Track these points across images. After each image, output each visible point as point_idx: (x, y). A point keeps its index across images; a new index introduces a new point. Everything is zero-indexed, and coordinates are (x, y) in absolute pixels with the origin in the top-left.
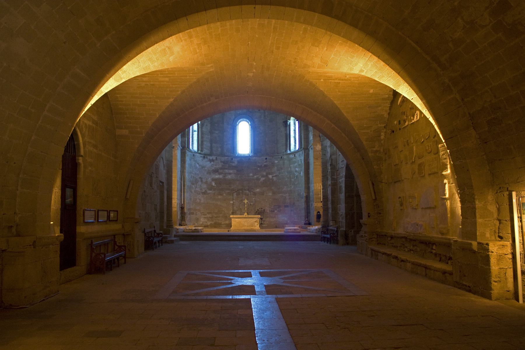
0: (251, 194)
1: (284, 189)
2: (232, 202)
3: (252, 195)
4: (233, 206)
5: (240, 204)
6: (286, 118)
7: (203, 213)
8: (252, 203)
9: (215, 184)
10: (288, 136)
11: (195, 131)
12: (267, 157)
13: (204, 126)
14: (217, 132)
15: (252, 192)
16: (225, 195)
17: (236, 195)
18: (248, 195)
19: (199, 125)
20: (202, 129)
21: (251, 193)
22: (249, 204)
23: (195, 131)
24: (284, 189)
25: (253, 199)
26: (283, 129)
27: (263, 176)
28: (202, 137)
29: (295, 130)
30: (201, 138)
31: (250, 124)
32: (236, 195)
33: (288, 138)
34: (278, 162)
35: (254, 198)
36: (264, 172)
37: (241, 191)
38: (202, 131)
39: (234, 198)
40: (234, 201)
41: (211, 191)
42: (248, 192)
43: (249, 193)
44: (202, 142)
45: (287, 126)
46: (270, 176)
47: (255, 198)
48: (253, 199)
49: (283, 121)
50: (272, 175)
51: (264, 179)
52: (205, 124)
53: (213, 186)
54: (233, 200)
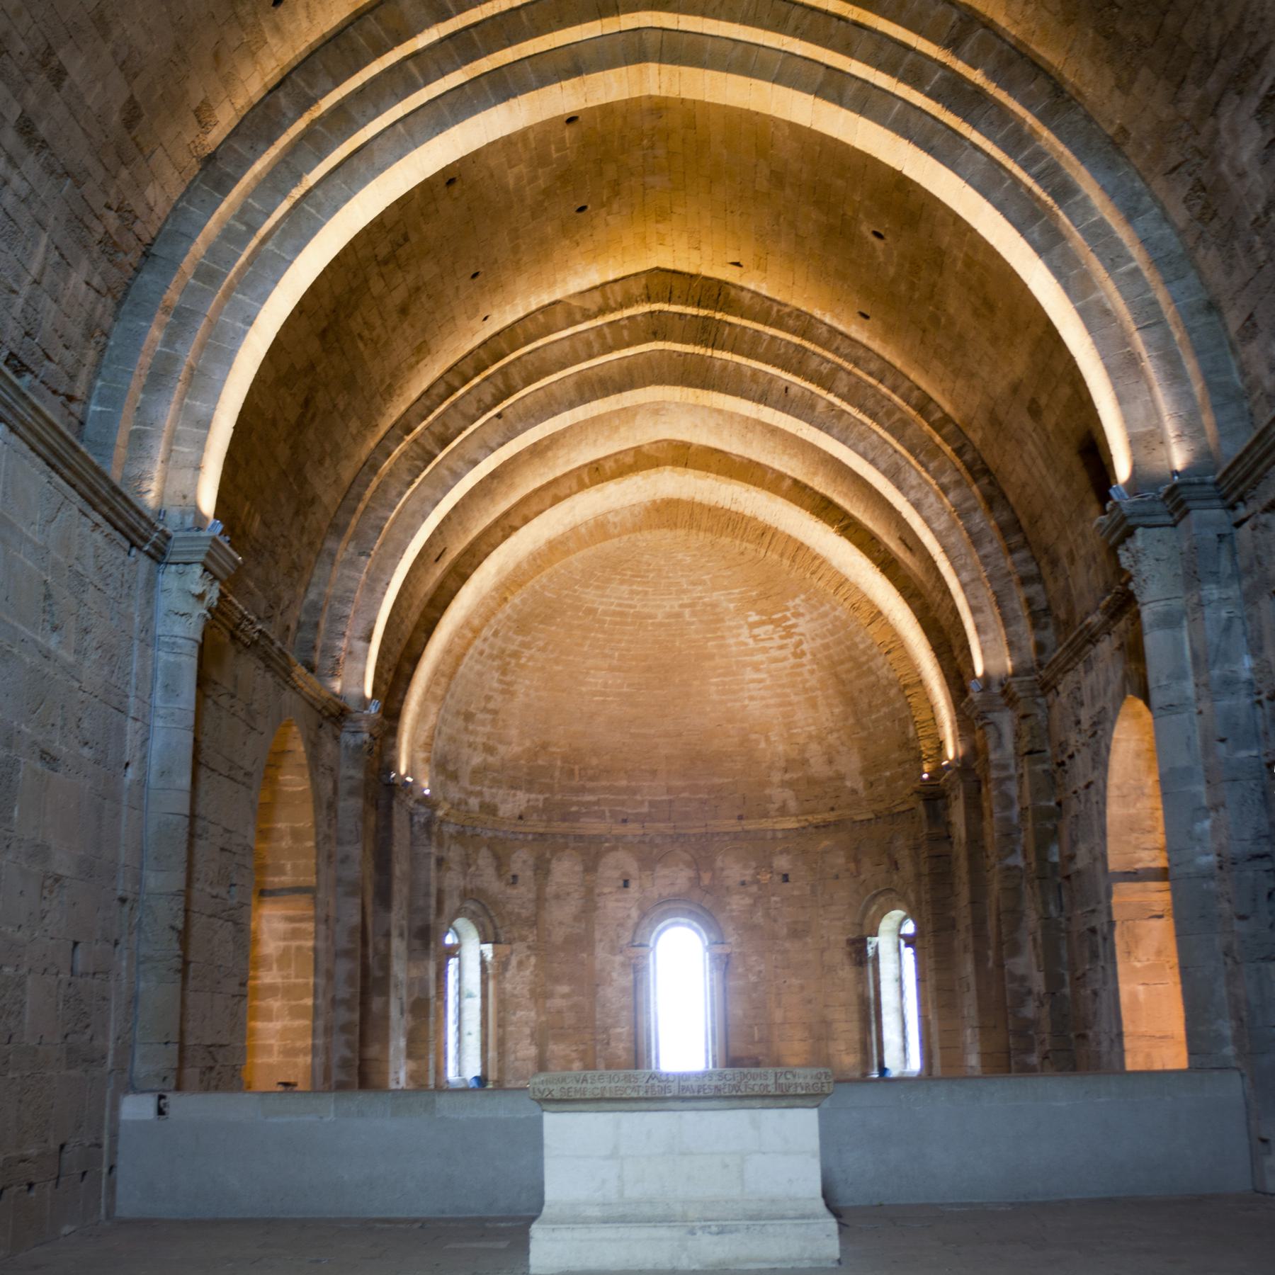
6: (861, 925)
10: (872, 1007)
11: (470, 996)
13: (510, 967)
14: (565, 989)
19: (489, 967)
20: (499, 983)
23: (470, 996)
26: (847, 972)
28: (501, 1024)
29: (900, 980)
30: (499, 1026)
33: (873, 1019)
38: (500, 992)
44: (501, 1042)
45: (866, 962)
49: (845, 938)
52: (514, 961)
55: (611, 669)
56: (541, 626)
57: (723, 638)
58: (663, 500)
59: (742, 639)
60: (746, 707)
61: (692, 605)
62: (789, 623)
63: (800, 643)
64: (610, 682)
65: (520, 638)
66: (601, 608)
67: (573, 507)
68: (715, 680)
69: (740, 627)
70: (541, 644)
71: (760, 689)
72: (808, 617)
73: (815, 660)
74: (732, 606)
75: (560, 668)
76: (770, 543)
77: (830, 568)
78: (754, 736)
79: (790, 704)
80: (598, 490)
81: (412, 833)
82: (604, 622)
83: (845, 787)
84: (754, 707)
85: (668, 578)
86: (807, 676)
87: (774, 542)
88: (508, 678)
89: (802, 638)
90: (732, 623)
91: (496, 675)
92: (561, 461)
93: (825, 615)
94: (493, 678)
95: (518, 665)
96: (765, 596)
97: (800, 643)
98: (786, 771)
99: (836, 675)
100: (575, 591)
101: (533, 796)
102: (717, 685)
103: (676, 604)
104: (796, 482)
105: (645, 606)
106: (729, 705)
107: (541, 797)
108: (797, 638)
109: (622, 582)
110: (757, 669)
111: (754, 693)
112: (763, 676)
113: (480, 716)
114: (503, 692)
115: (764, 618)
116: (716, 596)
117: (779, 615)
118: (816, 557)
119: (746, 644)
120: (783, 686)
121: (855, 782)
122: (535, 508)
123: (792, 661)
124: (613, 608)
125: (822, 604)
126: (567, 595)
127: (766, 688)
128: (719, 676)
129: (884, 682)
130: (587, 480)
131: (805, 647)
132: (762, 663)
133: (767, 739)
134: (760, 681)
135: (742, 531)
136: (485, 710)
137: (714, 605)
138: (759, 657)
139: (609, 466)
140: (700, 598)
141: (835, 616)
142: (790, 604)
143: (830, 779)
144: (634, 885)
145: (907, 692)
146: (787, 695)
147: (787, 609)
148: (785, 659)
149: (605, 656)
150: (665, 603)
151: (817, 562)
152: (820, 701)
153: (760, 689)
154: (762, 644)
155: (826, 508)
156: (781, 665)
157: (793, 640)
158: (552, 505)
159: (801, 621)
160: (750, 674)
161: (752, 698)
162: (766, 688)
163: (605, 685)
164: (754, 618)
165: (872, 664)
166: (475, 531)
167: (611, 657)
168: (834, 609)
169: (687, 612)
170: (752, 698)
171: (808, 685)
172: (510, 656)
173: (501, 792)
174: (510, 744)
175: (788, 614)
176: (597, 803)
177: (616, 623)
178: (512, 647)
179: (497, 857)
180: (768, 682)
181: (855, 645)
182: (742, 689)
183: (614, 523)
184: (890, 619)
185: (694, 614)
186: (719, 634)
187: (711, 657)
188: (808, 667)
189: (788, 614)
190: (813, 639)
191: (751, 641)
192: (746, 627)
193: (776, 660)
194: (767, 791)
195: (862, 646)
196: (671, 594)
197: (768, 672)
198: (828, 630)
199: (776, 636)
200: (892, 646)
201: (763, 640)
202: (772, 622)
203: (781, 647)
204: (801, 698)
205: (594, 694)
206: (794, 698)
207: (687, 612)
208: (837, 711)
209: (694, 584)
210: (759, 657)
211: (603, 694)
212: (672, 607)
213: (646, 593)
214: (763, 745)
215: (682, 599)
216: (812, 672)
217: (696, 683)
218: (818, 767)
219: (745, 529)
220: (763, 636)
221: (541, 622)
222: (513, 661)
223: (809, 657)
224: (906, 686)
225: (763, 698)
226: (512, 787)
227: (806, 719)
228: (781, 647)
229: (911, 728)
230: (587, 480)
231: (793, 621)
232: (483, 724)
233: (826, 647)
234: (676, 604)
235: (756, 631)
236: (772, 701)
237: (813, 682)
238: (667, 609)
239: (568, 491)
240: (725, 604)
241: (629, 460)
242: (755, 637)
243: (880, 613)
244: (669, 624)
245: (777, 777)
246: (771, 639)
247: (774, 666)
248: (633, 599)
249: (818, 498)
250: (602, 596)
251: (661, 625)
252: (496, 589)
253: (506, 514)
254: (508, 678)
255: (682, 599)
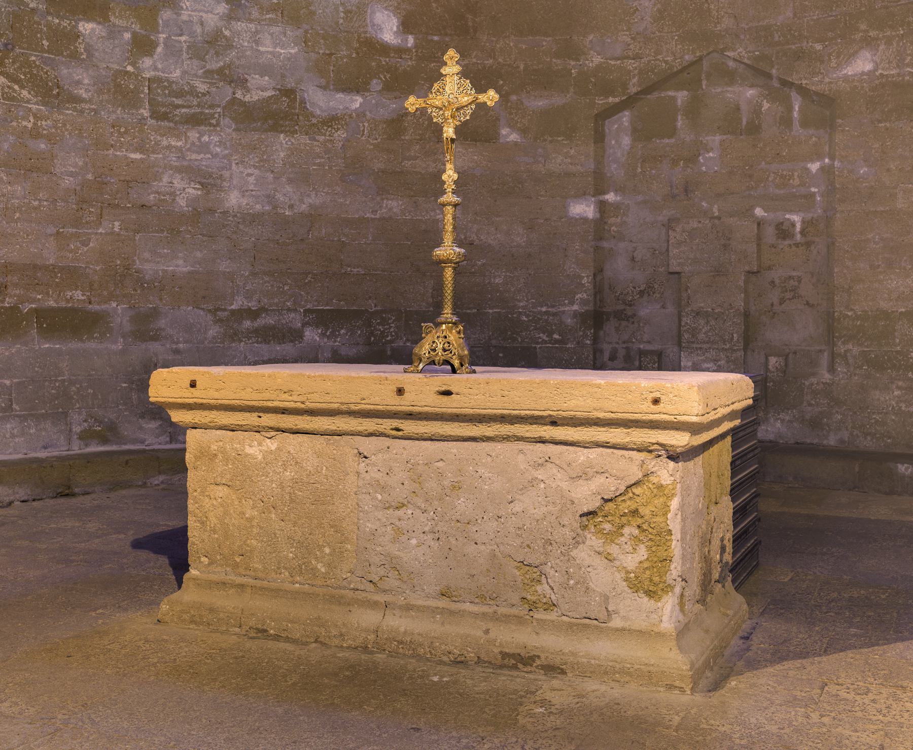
0: (786, 121)
2: (584, 209)
3: (797, 129)
4: (597, 249)
5: (669, 225)
7: (254, 314)
8: (796, 218)
9: (406, 26)
15: (803, 91)
16: (514, 137)
17: (635, 130)
18: (754, 129)
21: (790, 109)
22: (760, 223)
25: (814, 167)
32: (626, 141)
35: (820, 157)
37: (681, 96)
39: (614, 170)
40: (611, 197)
41: (357, 102)
42: (751, 92)
43: (766, 105)
47: (832, 158)
48: (814, 167)
53: (385, 49)
54: (599, 191)
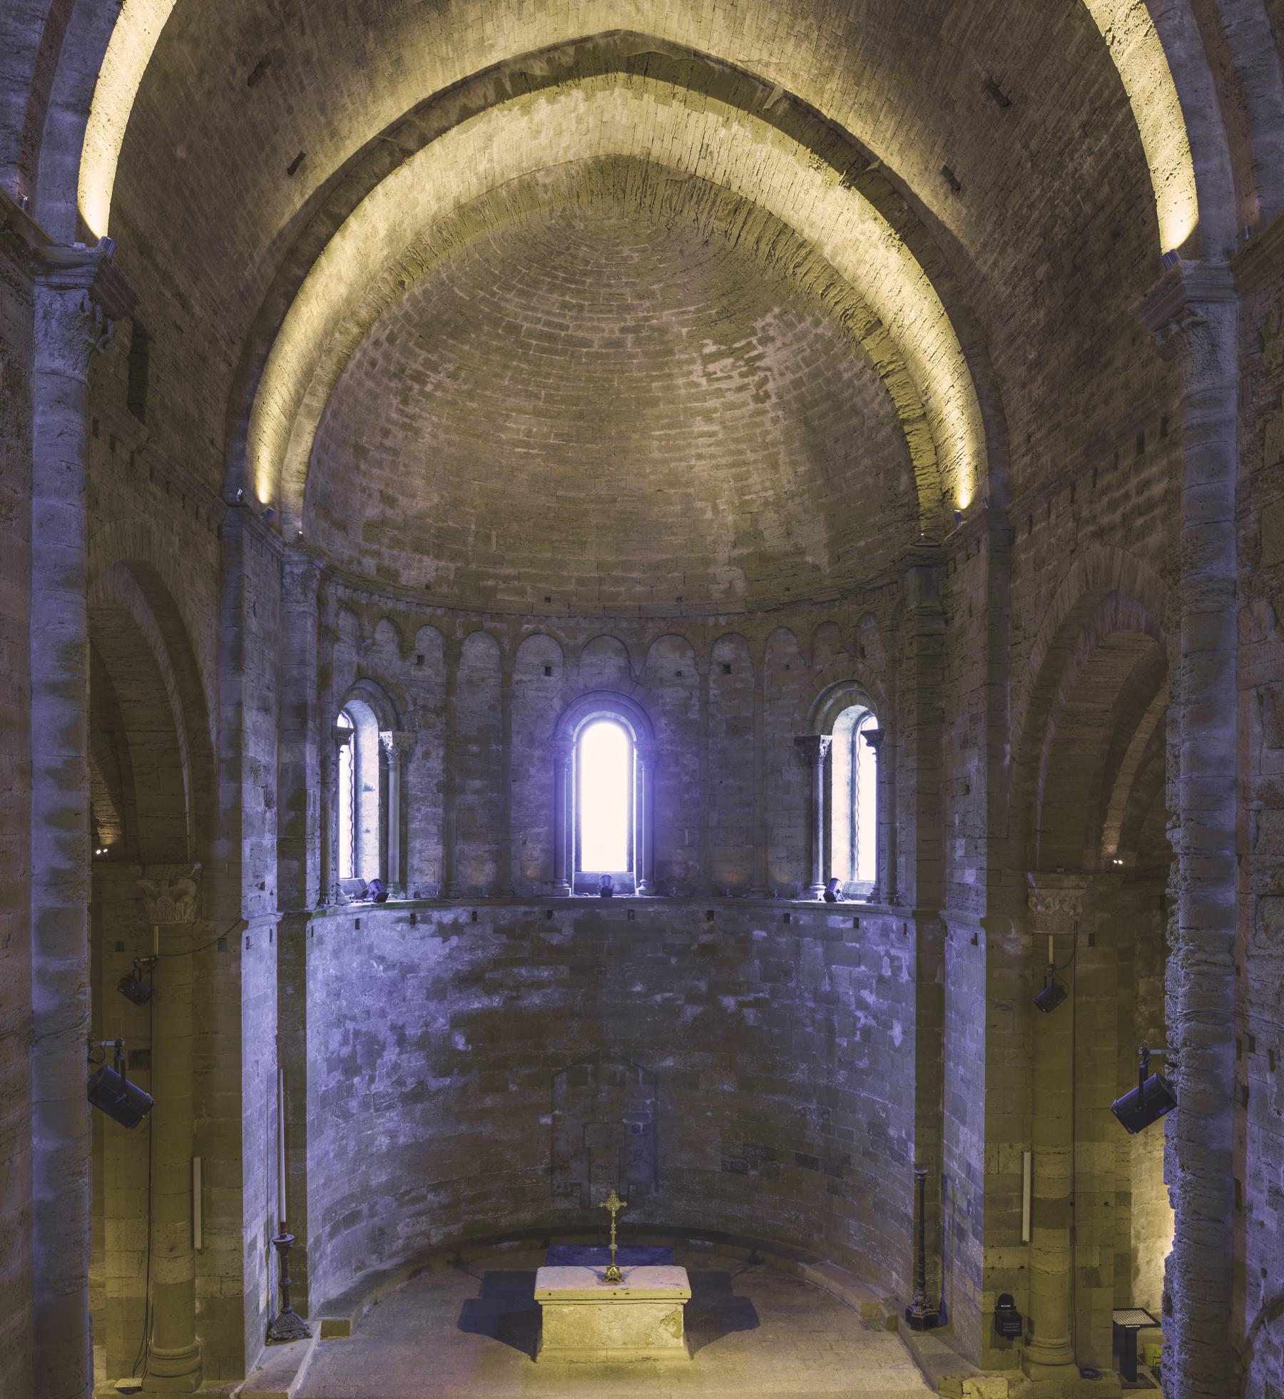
1: (799, 1076)
12: (717, 909)
24: (799, 1076)
27: (693, 998)
31: (635, 740)
34: (769, 938)
36: (698, 980)
46: (730, 1002)
50: (740, 998)
51: (698, 1010)
55: (537, 413)
56: (451, 341)
57: (670, 376)
58: (608, 156)
59: (694, 378)
60: (692, 467)
61: (635, 330)
62: (755, 353)
63: (765, 381)
64: (535, 430)
65: (424, 354)
66: (526, 325)
67: (489, 138)
68: (658, 433)
69: (692, 361)
70: (451, 367)
71: (710, 445)
72: (779, 343)
73: (781, 405)
74: (684, 331)
75: (474, 405)
76: (744, 223)
77: (821, 259)
78: (699, 504)
79: (745, 463)
80: (526, 110)
81: (282, 586)
82: (529, 346)
83: (806, 563)
84: (701, 467)
85: (609, 285)
86: (769, 426)
87: (750, 222)
88: (410, 410)
89: (768, 373)
90: (684, 357)
91: (395, 402)
92: (471, 36)
93: (803, 335)
94: (391, 405)
95: (422, 392)
96: (726, 314)
97: (765, 381)
98: (734, 546)
99: (806, 422)
100: (493, 294)
101: (442, 564)
102: (659, 439)
103: (616, 327)
104: (795, 102)
105: (579, 327)
106: (673, 465)
107: (452, 566)
108: (762, 374)
109: (552, 288)
110: (707, 416)
111: (703, 450)
112: (715, 428)
113: (377, 455)
114: (404, 427)
115: (723, 347)
116: (667, 316)
117: (743, 342)
118: (802, 245)
119: (697, 385)
120: (737, 441)
121: (818, 557)
122: (436, 125)
123: (752, 406)
124: (539, 327)
125: (801, 319)
126: (483, 299)
127: (718, 444)
128: (663, 427)
129: (871, 423)
130: (508, 87)
131: (770, 386)
132: (715, 410)
133: (715, 508)
134: (711, 434)
135: (709, 203)
136: (381, 447)
137: (663, 330)
138: (712, 403)
139: (539, 69)
140: (646, 319)
141: (816, 335)
142: (759, 324)
143: (787, 554)
144: (557, 673)
145: (907, 428)
146: (741, 452)
147: (754, 333)
148: (745, 404)
149: (530, 395)
150: (603, 325)
151: (803, 252)
152: (782, 457)
153: (710, 445)
154: (716, 385)
155: (833, 145)
156: (737, 412)
157: (756, 378)
158: (458, 122)
159: (770, 348)
160: (700, 426)
161: (700, 457)
162: (718, 444)
163: (529, 433)
164: (711, 348)
165: (858, 400)
166: (351, 147)
167: (537, 397)
168: (817, 323)
169: (630, 337)
170: (700, 457)
171: (769, 438)
172: (413, 378)
173: (403, 554)
174: (414, 497)
175: (754, 340)
176: (518, 577)
177: (544, 351)
178: (416, 366)
179: (399, 632)
180: (721, 436)
181: (838, 375)
182: (689, 445)
183: (545, 186)
184: (894, 331)
185: (638, 342)
186: (667, 371)
187: (655, 402)
188: (772, 414)
189: (754, 340)
190: (782, 374)
191: (704, 381)
192: (699, 361)
193: (731, 406)
194: (711, 571)
195: (846, 376)
196: (610, 311)
197: (722, 423)
198: (803, 359)
199: (735, 374)
200: (891, 367)
201: (718, 379)
202: (731, 352)
203: (741, 389)
204: (759, 456)
205: (516, 443)
206: (750, 456)
207: (630, 337)
208: (801, 469)
209: (640, 297)
210: (712, 403)
211: (527, 445)
212: (612, 331)
213: (581, 308)
214: (709, 515)
215: (625, 320)
216: (775, 420)
217: (636, 436)
218: (773, 540)
219: (714, 202)
220: (719, 374)
221: (451, 335)
222: (416, 387)
223: (774, 400)
224: (905, 421)
225: (713, 457)
226: (417, 550)
227: (763, 481)
228: (741, 389)
229: (905, 478)
230: (508, 87)
231: (760, 349)
232: (380, 465)
233: (797, 384)
234: (616, 327)
235: (711, 367)
236: (723, 461)
237: (776, 433)
238: (606, 335)
239: (482, 102)
240: (676, 329)
241: (567, 60)
242: (708, 375)
243: (879, 322)
244: (607, 356)
245: (723, 553)
246: (730, 377)
247: (728, 414)
248: (564, 316)
249: (824, 130)
250: (527, 308)
251: (598, 356)
252: (390, 270)
253: (395, 129)
254: (410, 410)
255: (625, 320)
